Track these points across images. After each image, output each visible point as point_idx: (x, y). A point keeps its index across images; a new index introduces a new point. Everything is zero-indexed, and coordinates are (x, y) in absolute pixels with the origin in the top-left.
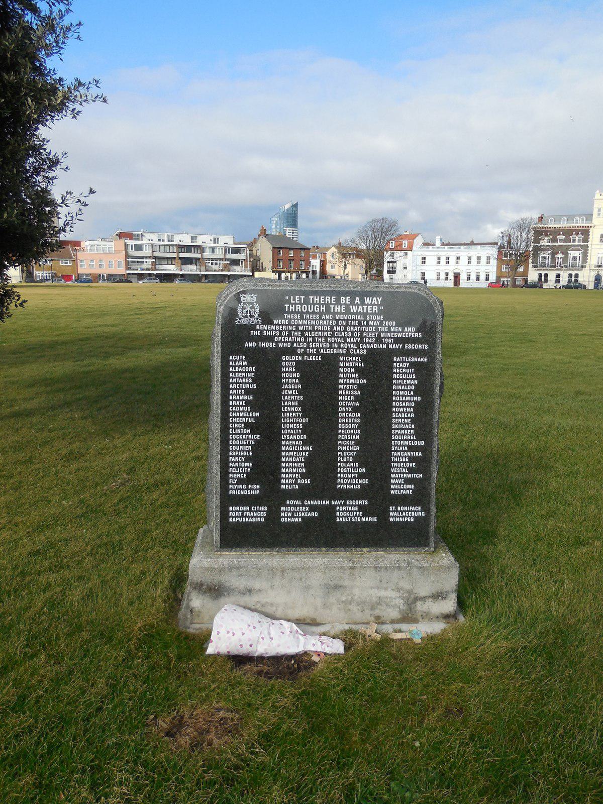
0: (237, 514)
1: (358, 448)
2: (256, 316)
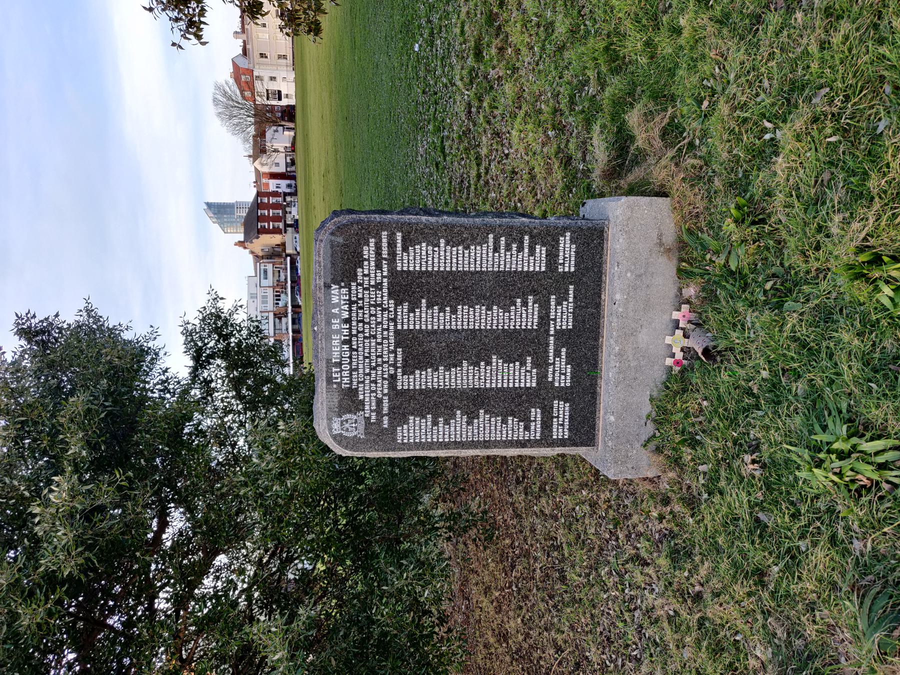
0: (560, 430)
1: (495, 307)
2: (355, 417)
